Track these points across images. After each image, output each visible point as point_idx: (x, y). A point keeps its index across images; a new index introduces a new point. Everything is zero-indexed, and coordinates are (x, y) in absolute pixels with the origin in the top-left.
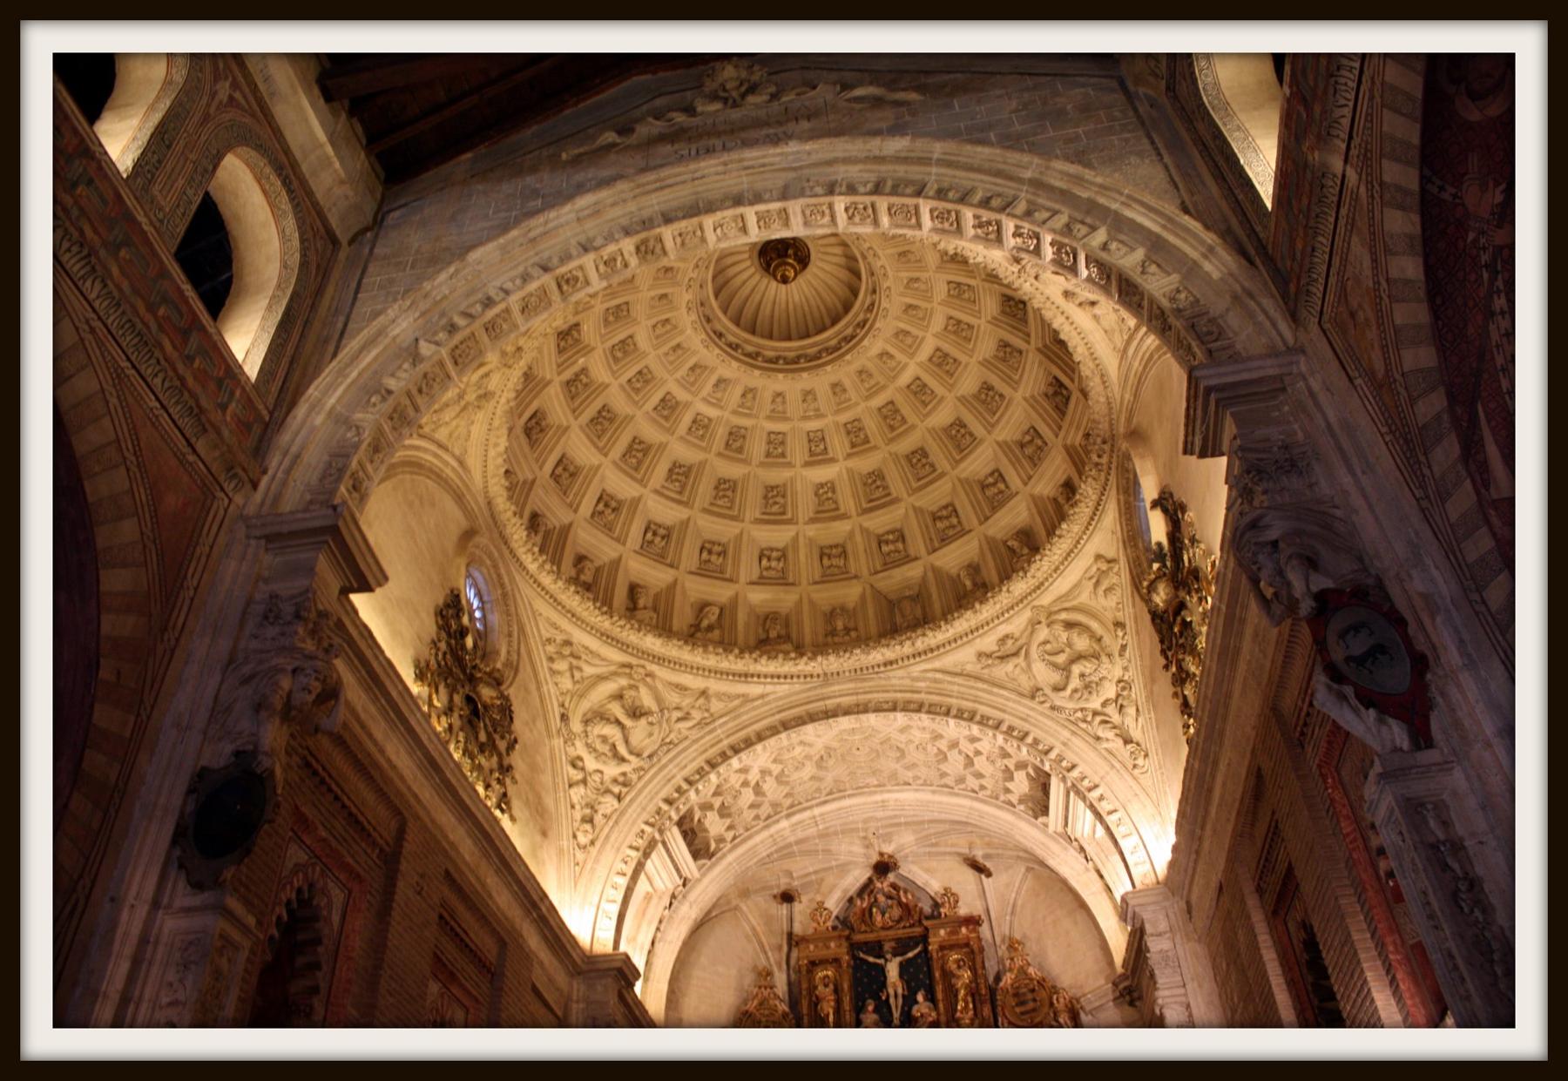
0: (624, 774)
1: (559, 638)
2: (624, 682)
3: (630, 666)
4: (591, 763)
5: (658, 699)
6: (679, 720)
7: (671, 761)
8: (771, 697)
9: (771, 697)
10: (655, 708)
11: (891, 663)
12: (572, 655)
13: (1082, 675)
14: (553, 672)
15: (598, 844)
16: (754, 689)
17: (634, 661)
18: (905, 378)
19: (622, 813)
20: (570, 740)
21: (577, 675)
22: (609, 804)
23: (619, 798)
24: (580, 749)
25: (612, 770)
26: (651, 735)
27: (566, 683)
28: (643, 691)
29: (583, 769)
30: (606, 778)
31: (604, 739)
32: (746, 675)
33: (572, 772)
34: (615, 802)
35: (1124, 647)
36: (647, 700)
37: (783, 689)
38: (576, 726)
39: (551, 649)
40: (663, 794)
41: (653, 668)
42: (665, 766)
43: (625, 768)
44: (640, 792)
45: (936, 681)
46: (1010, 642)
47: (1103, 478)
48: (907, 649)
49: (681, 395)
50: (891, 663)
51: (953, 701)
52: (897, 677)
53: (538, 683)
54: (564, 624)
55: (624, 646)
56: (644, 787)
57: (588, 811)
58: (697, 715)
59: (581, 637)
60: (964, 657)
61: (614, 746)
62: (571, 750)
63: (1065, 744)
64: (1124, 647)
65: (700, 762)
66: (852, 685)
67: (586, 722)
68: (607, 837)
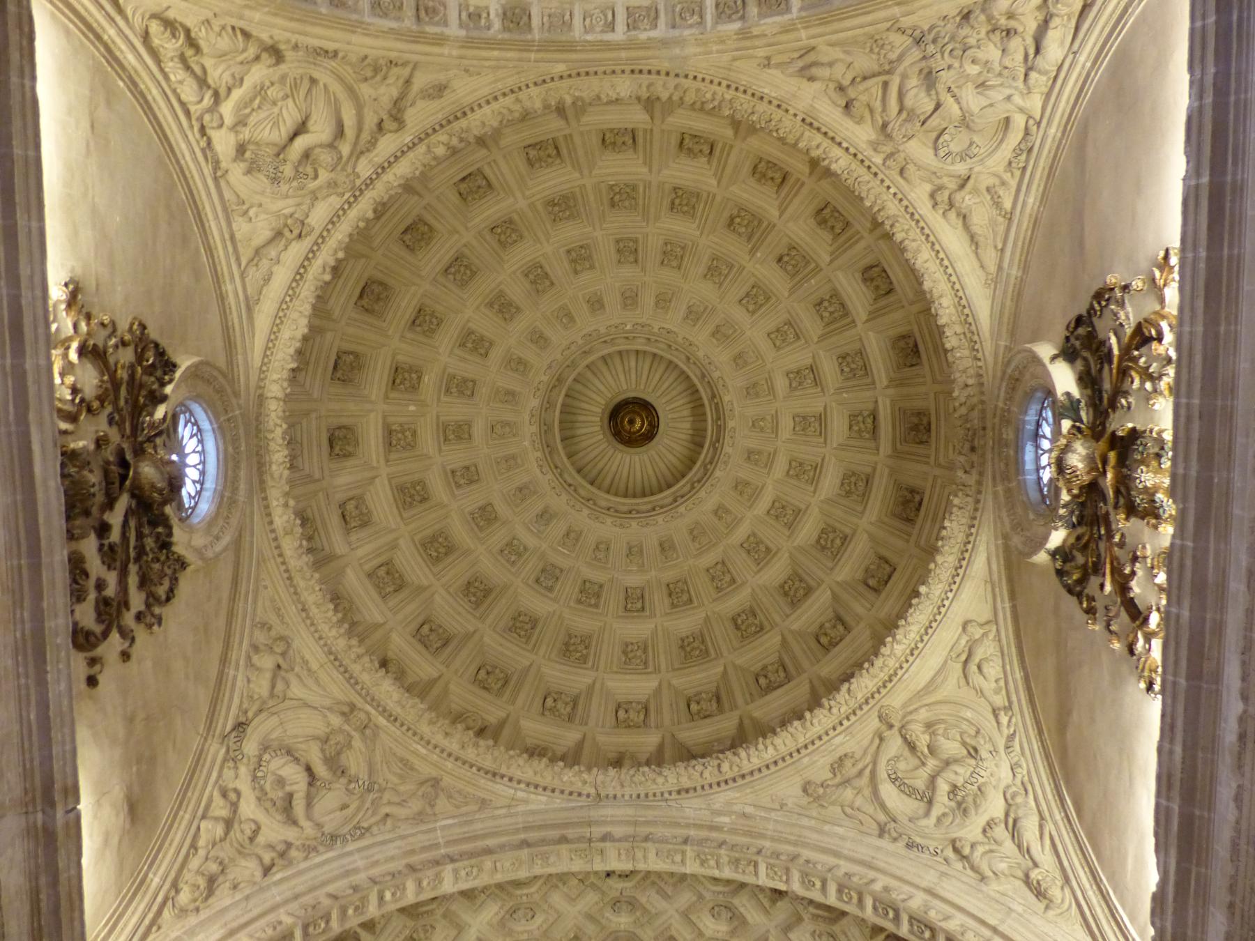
0: (289, 845)
1: (278, 629)
2: (336, 721)
3: (353, 707)
4: (249, 808)
5: (371, 772)
6: (389, 803)
7: (359, 850)
8: (521, 808)
9: (521, 808)
10: (364, 775)
11: (687, 791)
12: (283, 654)
13: (954, 789)
14: (250, 663)
15: (203, 915)
16: (502, 790)
17: (359, 702)
18: (741, 532)
19: (262, 890)
20: (233, 758)
21: (280, 686)
22: (248, 869)
23: (267, 871)
24: (244, 785)
25: (274, 831)
26: (344, 807)
27: (262, 686)
28: (357, 743)
29: (235, 806)
30: (261, 839)
31: (281, 782)
32: (494, 775)
33: (218, 801)
34: (258, 873)
35: (1011, 737)
36: (355, 762)
37: (539, 801)
38: (251, 747)
39: (261, 637)
40: (331, 889)
41: (382, 721)
42: (350, 854)
43: (291, 834)
44: (300, 873)
45: (744, 815)
46: (848, 763)
47: (971, 507)
48: (710, 774)
49: (502, 509)
50: (687, 791)
51: (767, 844)
52: (692, 808)
53: (224, 660)
54: (292, 610)
55: (353, 681)
56: (309, 869)
57: (214, 867)
58: (415, 805)
59: (307, 647)
60: (787, 787)
61: (290, 796)
62: (228, 773)
63: (929, 891)
64: (1011, 737)
65: (398, 865)
66: (630, 811)
67: (265, 748)
68: (224, 911)
